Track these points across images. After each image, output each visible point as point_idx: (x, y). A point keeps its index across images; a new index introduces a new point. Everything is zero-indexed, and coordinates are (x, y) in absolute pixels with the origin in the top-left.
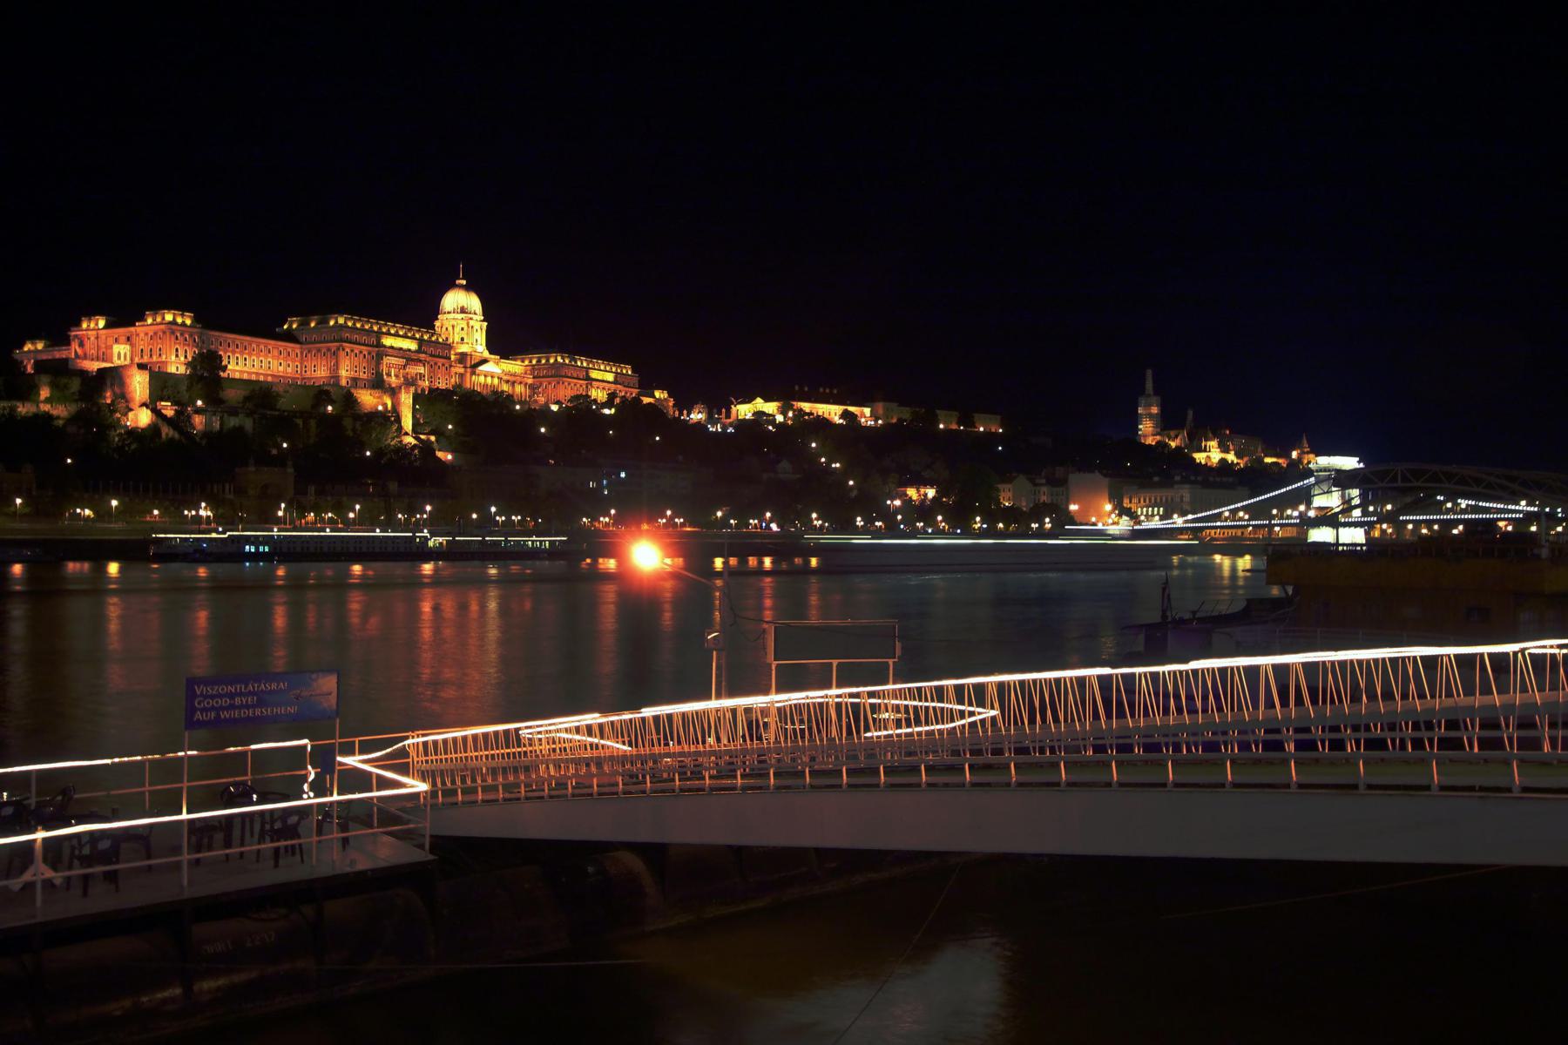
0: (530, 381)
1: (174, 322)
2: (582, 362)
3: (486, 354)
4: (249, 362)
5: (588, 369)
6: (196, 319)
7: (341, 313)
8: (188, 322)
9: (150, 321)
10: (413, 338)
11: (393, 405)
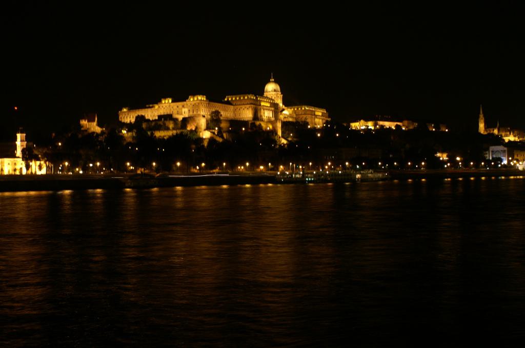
0: (295, 116)
1: (201, 100)
2: (312, 109)
3: (284, 107)
4: (227, 113)
5: (314, 111)
6: (207, 98)
7: (249, 94)
8: (205, 99)
9: (192, 99)
10: (268, 102)
11: (273, 127)
